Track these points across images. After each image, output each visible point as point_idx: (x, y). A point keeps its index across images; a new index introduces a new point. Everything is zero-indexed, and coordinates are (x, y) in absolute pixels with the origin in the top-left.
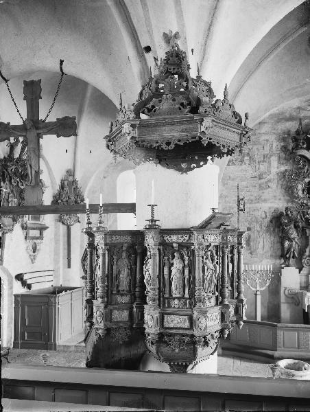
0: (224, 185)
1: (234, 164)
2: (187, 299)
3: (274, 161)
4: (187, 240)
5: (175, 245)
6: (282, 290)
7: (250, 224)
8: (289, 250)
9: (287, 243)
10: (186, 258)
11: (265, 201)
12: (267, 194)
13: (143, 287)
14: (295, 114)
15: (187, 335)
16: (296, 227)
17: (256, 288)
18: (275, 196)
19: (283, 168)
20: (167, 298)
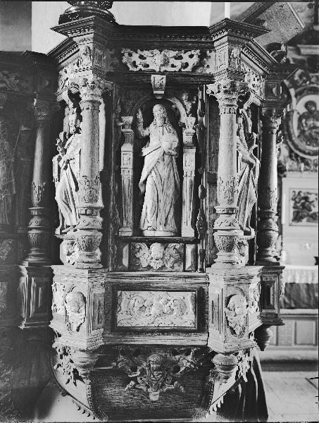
2: (187, 242)
4: (195, 68)
5: (158, 80)
10: (188, 121)
13: (51, 214)
15: (187, 350)
20: (127, 240)
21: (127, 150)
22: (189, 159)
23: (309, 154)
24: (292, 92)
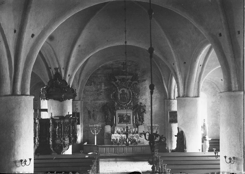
0: (84, 94)
1: (88, 85)
3: (103, 85)
6: (105, 133)
7: (94, 109)
8: (107, 118)
9: (107, 116)
11: (100, 100)
12: (101, 97)
14: (110, 66)
16: (110, 110)
17: (94, 133)
18: (103, 98)
19: (106, 88)
21: (55, 128)
22: (60, 130)
23: (123, 104)
24: (118, 88)
